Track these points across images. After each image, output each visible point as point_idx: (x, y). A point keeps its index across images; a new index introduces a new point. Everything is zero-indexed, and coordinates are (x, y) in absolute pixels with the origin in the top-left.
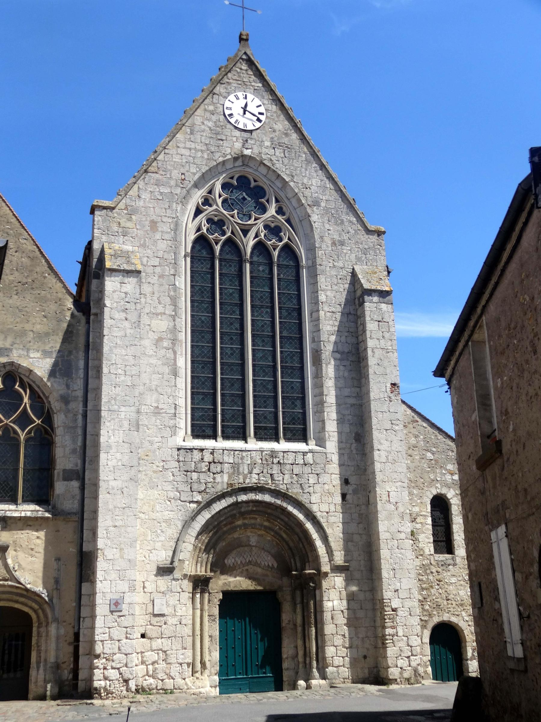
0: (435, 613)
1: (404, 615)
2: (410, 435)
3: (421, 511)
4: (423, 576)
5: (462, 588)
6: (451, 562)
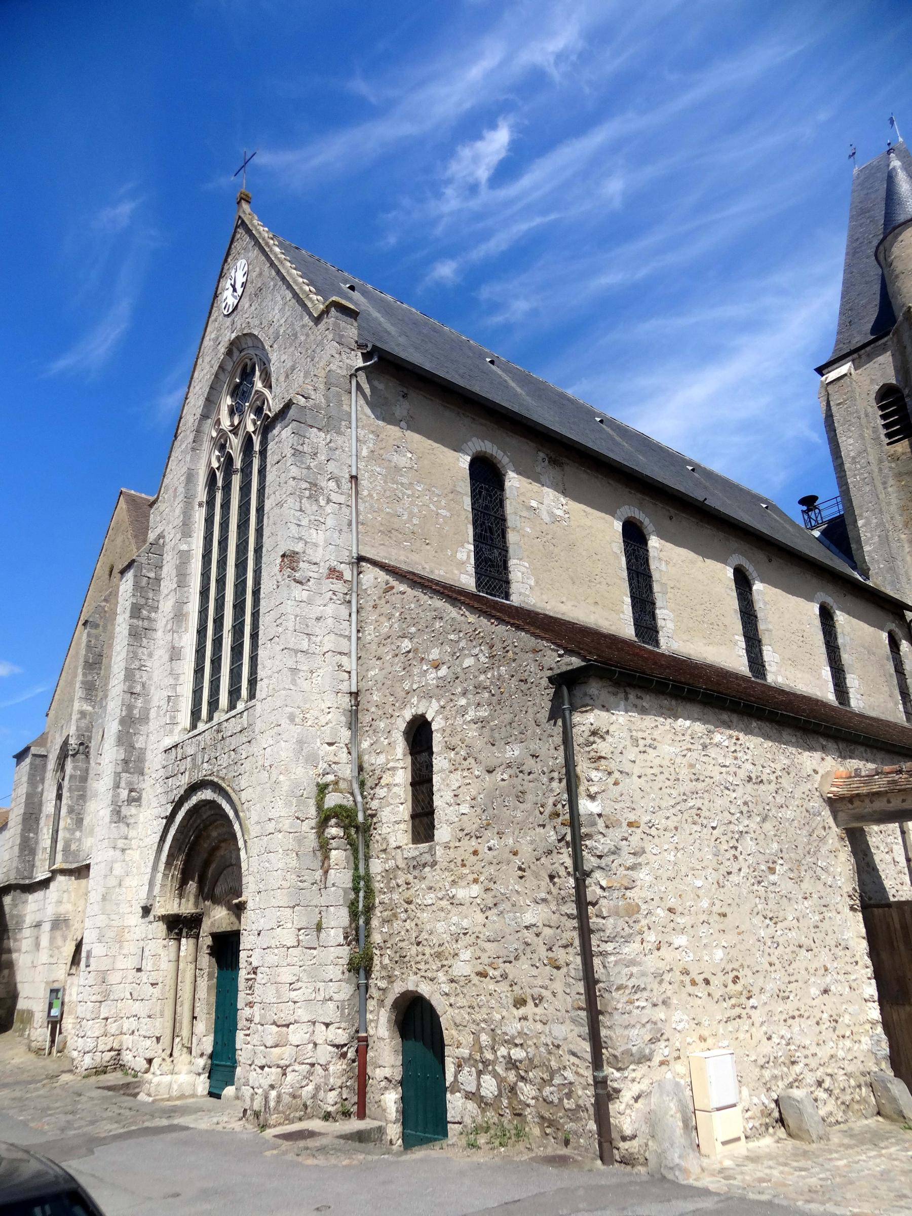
0: (396, 973)
1: (263, 982)
2: (383, 619)
3: (388, 761)
4: (385, 893)
5: (443, 914)
6: (427, 858)
